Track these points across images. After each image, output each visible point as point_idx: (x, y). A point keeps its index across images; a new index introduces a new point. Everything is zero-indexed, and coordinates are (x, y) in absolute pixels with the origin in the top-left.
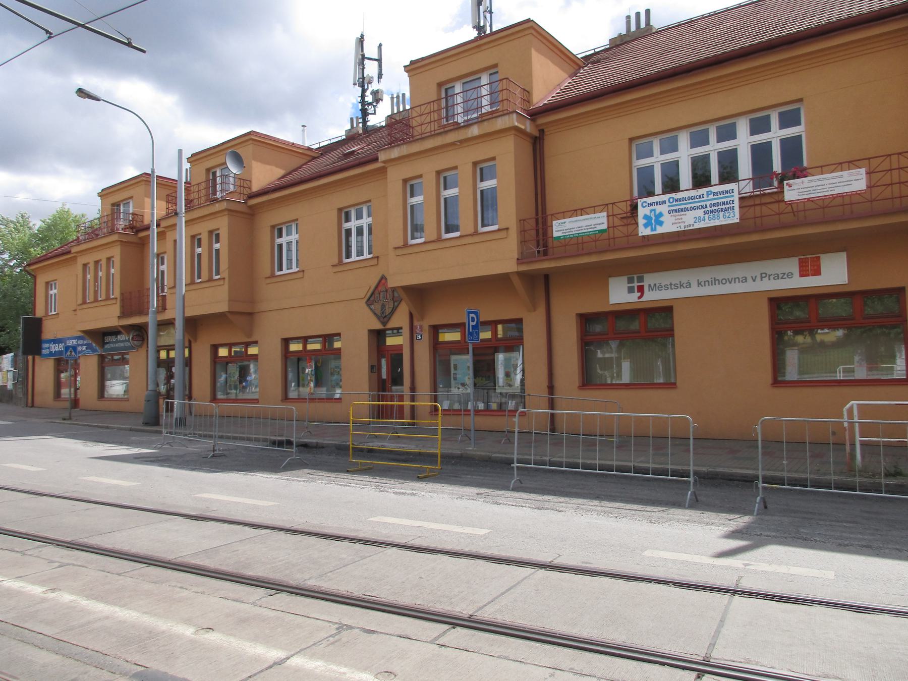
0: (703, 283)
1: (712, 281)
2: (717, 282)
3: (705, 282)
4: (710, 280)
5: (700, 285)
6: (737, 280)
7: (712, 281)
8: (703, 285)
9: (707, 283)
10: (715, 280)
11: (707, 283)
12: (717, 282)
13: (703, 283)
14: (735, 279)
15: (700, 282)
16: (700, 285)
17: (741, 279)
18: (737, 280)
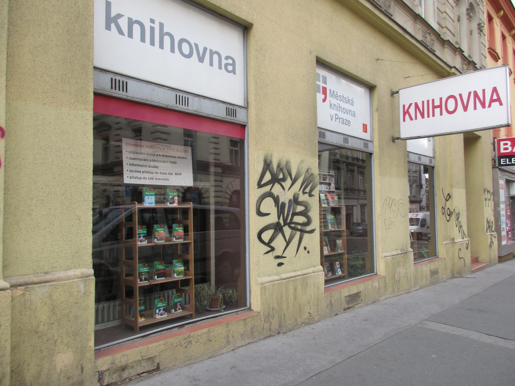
0: (123, 23)
1: (152, 29)
2: (167, 40)
3: (131, 22)
4: (148, 26)
5: (113, 26)
6: (215, 57)
7: (152, 29)
8: (125, 29)
9: (136, 28)
10: (162, 35)
11: (136, 28)
12: (167, 40)
13: (123, 23)
14: (212, 53)
15: (113, 14)
16: (113, 26)
17: (224, 62)
18: (215, 57)
